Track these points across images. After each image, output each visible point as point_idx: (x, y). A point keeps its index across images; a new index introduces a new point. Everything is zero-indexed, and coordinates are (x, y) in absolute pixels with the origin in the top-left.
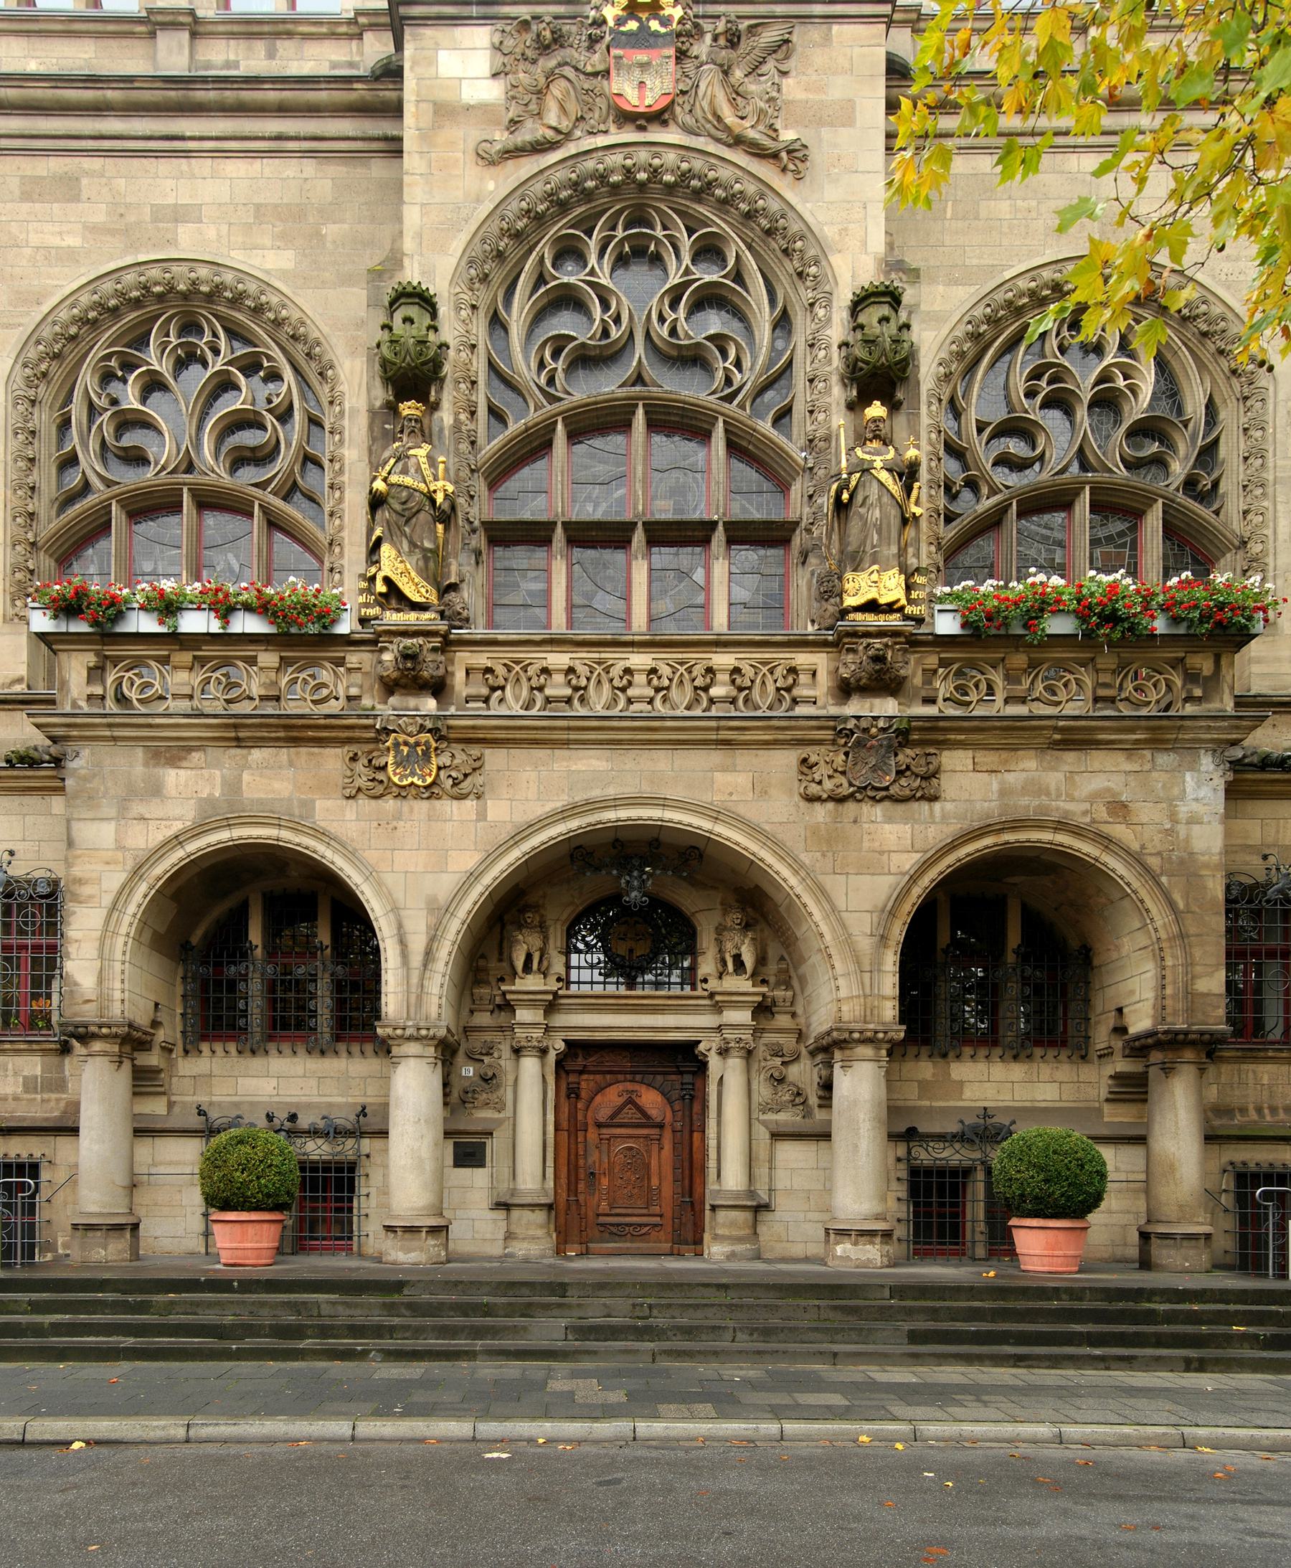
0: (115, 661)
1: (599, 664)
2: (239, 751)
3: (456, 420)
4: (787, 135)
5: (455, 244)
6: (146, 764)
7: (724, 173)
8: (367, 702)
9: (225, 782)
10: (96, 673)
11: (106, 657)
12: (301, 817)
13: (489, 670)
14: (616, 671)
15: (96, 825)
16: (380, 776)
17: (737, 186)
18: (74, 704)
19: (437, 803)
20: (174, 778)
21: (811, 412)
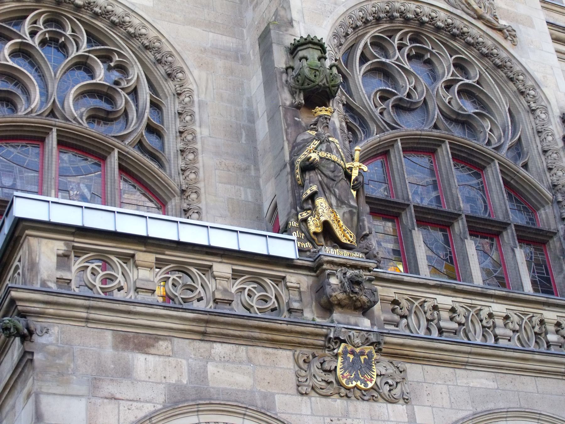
0: (79, 252)
1: (470, 307)
2: (203, 344)
3: (341, 125)
4: (503, 22)
5: (325, 23)
6: (115, 347)
7: (474, 31)
8: (308, 315)
9: (191, 371)
10: (63, 259)
11: (74, 248)
12: (263, 408)
13: (395, 302)
14: (484, 314)
15: (66, 400)
16: (331, 378)
17: (481, 40)
18: (44, 283)
19: (375, 404)
20: (142, 362)
21: (550, 169)
